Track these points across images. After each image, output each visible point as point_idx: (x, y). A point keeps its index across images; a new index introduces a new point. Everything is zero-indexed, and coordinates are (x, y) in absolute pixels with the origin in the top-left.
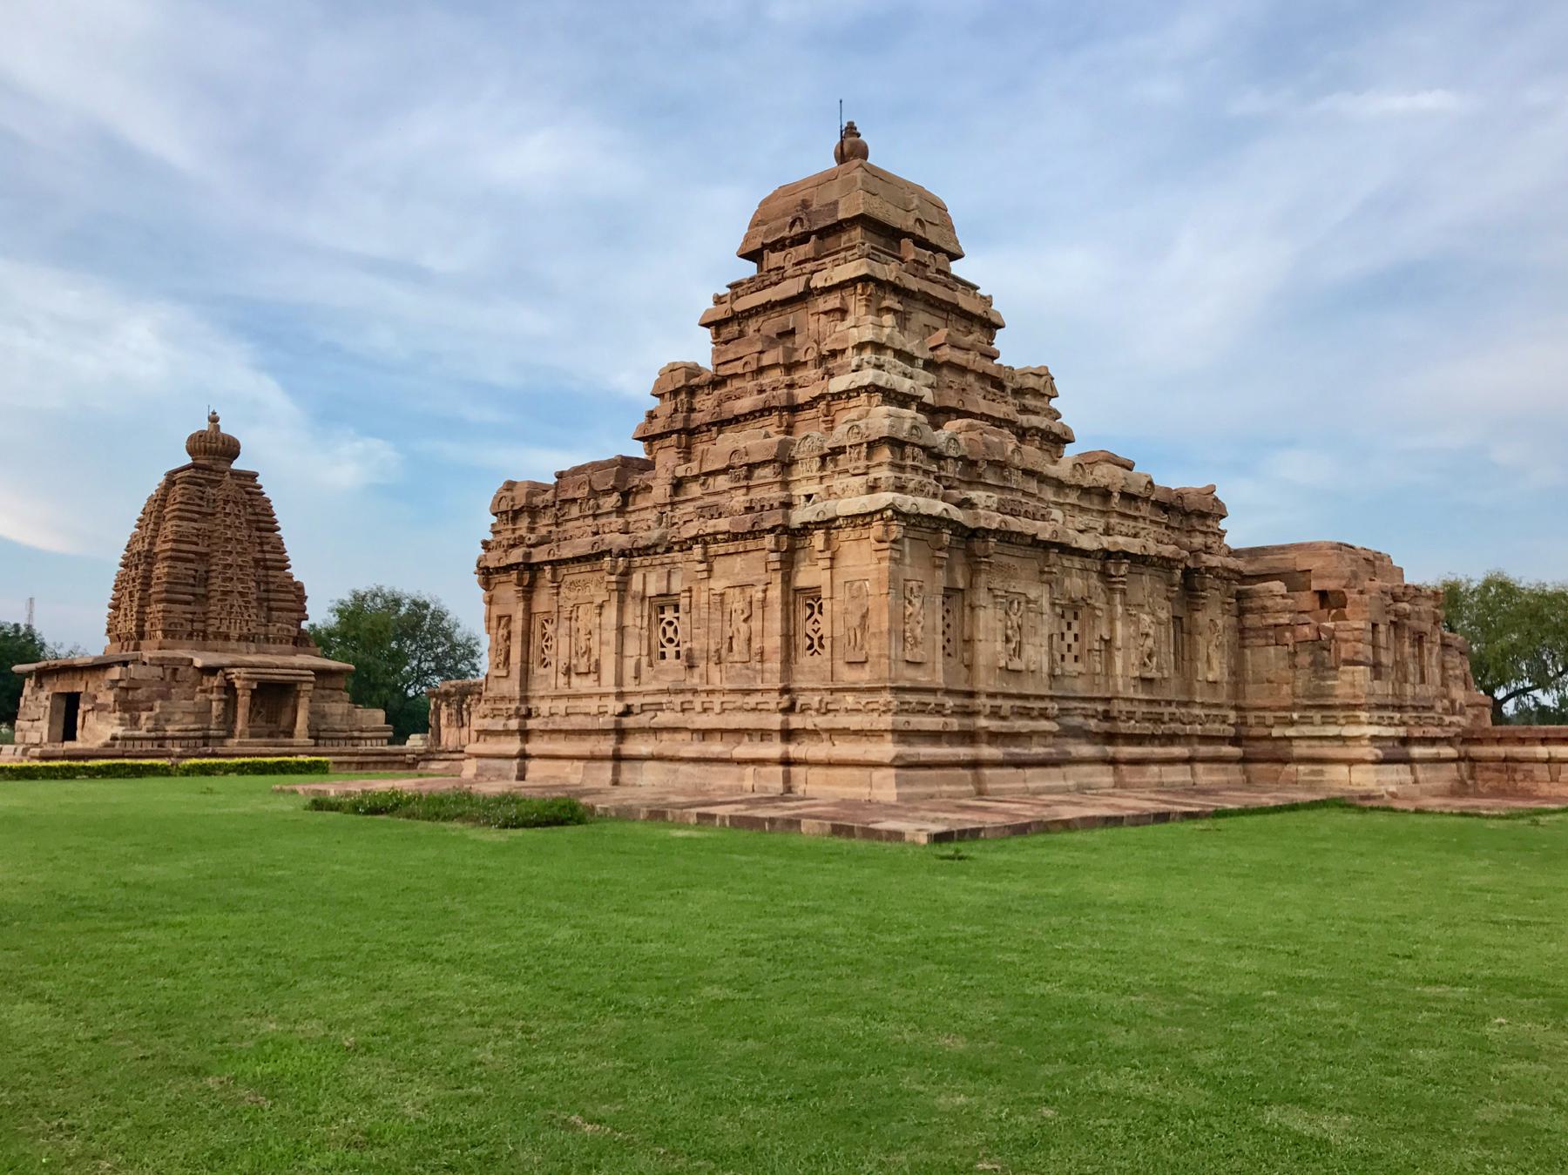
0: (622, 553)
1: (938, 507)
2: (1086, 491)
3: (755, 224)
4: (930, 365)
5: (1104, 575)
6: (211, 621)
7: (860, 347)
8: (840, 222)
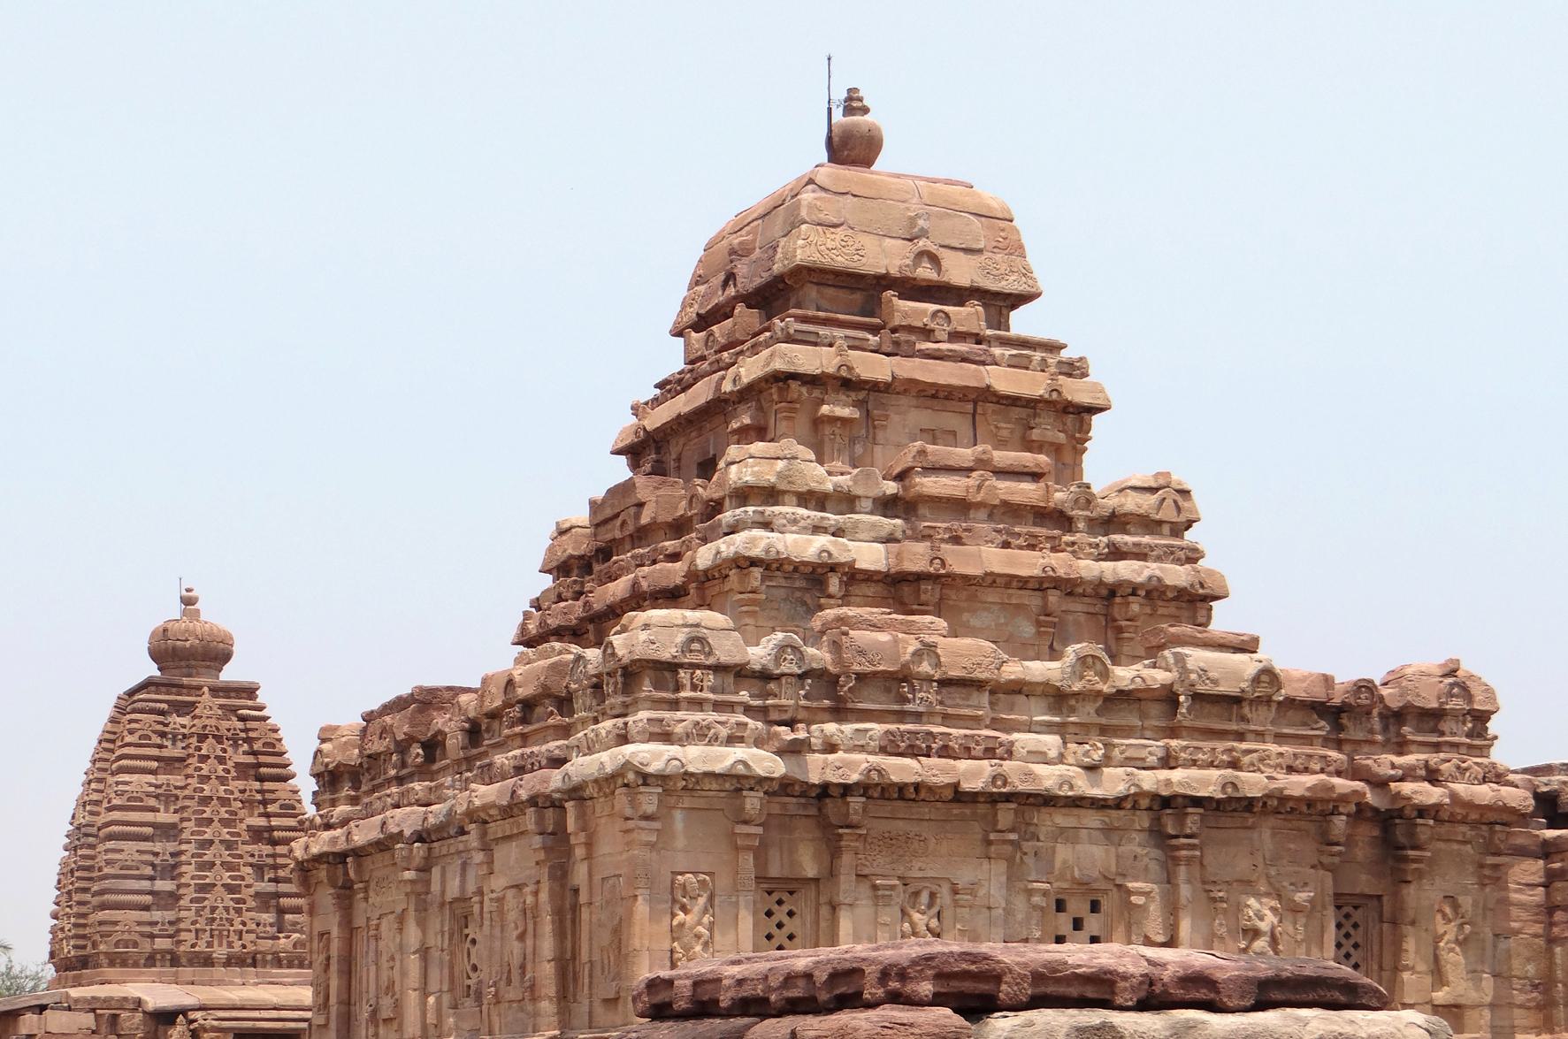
0: (420, 837)
1: (726, 758)
2: (1123, 697)
3: (698, 280)
4: (887, 505)
5: (1159, 836)
6: (183, 936)
7: (744, 495)
8: (780, 278)
